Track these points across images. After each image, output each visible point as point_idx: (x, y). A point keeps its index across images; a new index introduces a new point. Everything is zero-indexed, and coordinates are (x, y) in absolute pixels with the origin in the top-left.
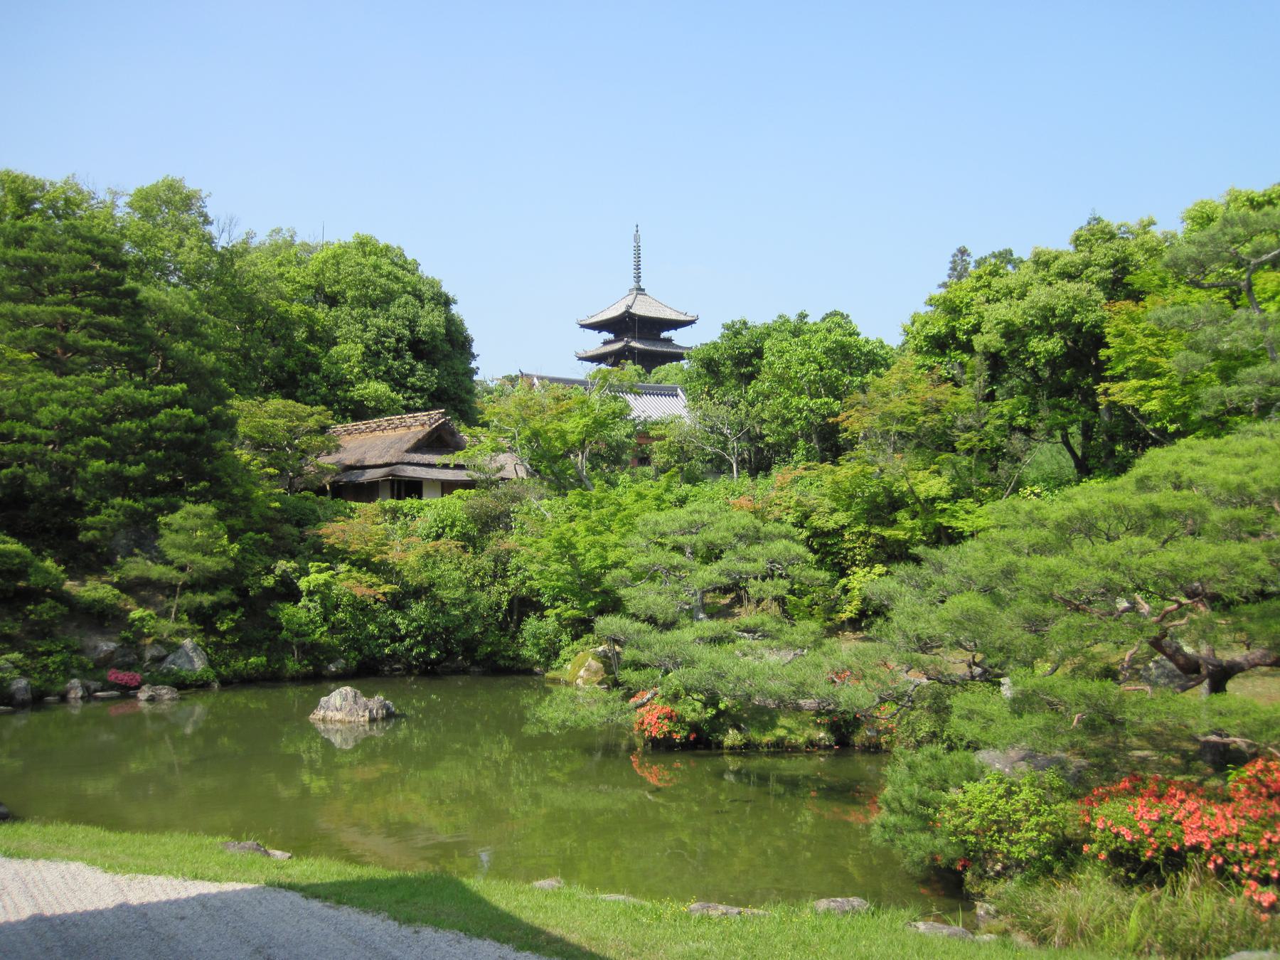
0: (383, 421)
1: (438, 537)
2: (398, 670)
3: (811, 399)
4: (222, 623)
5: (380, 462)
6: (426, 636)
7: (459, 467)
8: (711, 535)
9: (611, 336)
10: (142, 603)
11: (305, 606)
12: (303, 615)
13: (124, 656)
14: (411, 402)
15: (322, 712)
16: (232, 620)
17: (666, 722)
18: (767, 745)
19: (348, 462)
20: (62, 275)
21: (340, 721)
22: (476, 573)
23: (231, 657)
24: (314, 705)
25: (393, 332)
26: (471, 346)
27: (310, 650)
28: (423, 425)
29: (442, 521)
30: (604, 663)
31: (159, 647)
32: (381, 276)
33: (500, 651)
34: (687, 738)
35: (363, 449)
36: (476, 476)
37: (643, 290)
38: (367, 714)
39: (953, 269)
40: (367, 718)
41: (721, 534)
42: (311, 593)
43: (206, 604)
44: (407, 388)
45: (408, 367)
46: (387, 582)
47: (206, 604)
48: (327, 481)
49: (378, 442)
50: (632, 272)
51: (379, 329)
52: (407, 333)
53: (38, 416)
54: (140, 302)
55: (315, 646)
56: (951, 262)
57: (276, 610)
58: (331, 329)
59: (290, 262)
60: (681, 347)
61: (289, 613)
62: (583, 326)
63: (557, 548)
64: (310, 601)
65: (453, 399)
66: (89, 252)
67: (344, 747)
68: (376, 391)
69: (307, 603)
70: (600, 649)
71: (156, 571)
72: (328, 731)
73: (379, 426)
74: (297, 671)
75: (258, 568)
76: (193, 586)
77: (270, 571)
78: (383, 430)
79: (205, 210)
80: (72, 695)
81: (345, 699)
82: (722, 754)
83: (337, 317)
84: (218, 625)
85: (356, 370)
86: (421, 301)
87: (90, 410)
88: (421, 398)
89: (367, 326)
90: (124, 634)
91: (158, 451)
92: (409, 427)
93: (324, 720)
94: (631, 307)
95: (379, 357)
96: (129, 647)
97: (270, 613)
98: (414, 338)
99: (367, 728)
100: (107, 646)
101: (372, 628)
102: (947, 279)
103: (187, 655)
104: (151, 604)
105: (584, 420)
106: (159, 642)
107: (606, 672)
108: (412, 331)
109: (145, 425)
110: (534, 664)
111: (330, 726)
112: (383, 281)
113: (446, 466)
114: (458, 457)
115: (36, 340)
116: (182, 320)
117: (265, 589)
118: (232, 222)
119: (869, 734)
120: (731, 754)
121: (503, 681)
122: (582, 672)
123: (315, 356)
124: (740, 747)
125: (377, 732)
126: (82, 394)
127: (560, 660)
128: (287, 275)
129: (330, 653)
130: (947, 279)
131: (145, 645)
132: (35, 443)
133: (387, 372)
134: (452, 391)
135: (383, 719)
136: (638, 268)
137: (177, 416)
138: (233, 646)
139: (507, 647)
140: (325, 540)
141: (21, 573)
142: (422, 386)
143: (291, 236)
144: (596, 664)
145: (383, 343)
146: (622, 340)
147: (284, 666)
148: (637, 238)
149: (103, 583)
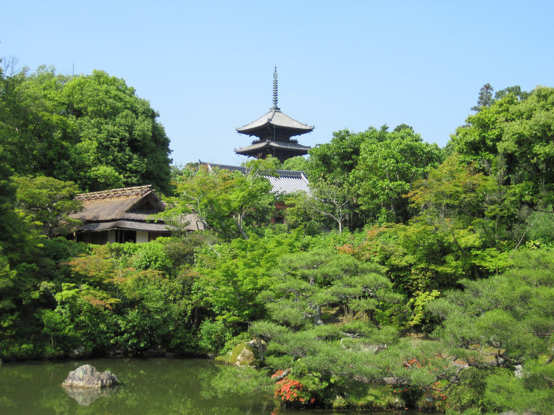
0: (111, 192)
1: (147, 268)
3: (391, 182)
4: (5, 322)
5: (109, 218)
7: (160, 222)
8: (326, 269)
9: (258, 139)
11: (59, 312)
12: (57, 317)
14: (129, 180)
15: (70, 381)
16: (11, 320)
17: (296, 390)
18: (361, 406)
19: (87, 218)
21: (82, 387)
22: (171, 292)
23: (10, 344)
24: (65, 376)
25: (118, 134)
26: (168, 144)
28: (137, 195)
29: (149, 258)
30: (254, 351)
32: (110, 98)
33: (185, 343)
34: (309, 401)
35: (98, 210)
36: (171, 228)
37: (279, 109)
38: (100, 383)
39: (481, 98)
40: (99, 385)
41: (333, 269)
42: (63, 303)
44: (127, 170)
46: (113, 297)
48: (74, 230)
49: (108, 205)
50: (272, 97)
51: (109, 132)
55: (65, 337)
56: (480, 94)
57: (41, 314)
58: (77, 131)
59: (51, 87)
60: (302, 146)
61: (48, 315)
62: (240, 132)
63: (225, 276)
64: (63, 308)
65: (156, 179)
67: (84, 404)
68: (105, 172)
69: (61, 309)
70: (251, 342)
72: (74, 393)
73: (108, 195)
74: (53, 354)
75: (29, 286)
77: (36, 288)
78: (111, 198)
81: (85, 373)
82: (332, 412)
83: (81, 124)
84: (2, 323)
85: (92, 158)
86: (136, 114)
88: (136, 177)
89: (101, 130)
92: (128, 196)
93: (71, 386)
94: (271, 120)
95: (109, 150)
97: (36, 316)
99: (100, 392)
101: (102, 326)
102: (477, 105)
108: (131, 134)
110: (208, 351)
111: (75, 391)
113: (152, 222)
114: (160, 216)
117: (34, 300)
118: (14, 61)
119: (428, 400)
120: (338, 412)
121: (187, 362)
122: (239, 357)
123: (67, 148)
124: (343, 408)
125: (106, 394)
127: (225, 349)
128: (49, 96)
129: (74, 342)
130: (477, 105)
133: (114, 160)
134: (156, 173)
135: (110, 386)
136: (276, 95)
138: (11, 337)
139: (190, 340)
140: (73, 269)
143: (52, 71)
144: (248, 352)
145: (113, 140)
146: (265, 141)
147: (44, 350)
148: (275, 76)
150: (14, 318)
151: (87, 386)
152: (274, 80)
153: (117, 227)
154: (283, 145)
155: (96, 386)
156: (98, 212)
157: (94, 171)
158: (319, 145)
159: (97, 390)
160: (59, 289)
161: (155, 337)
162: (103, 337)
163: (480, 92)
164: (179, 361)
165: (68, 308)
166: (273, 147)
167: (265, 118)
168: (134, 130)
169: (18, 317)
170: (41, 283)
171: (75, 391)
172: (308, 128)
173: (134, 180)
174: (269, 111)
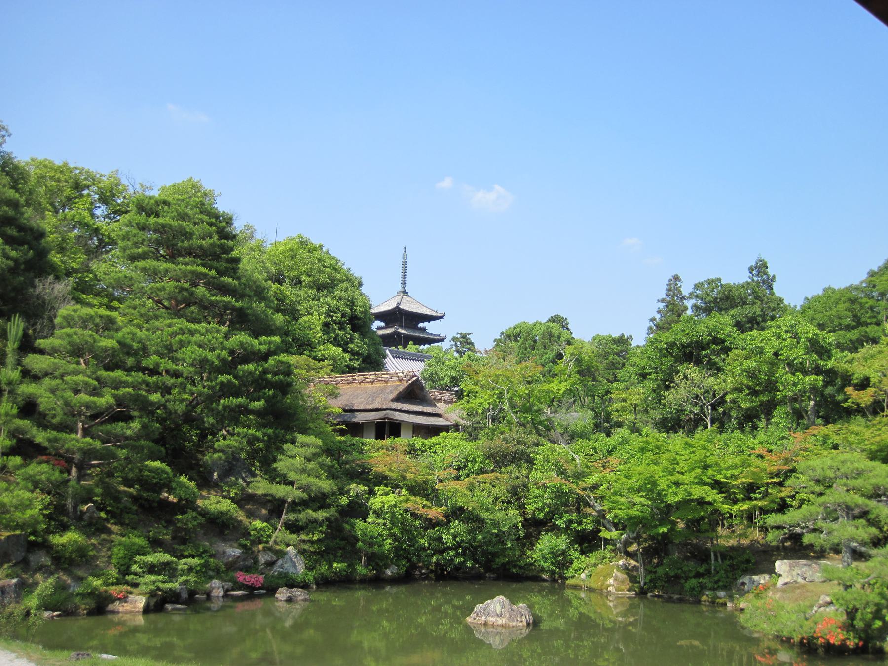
2: (424, 574)
5: (370, 407)
9: (383, 324)
10: (251, 515)
13: (244, 560)
15: (484, 618)
20: (195, 242)
22: (497, 499)
27: (374, 559)
28: (400, 381)
30: (628, 574)
31: (270, 554)
32: (325, 267)
37: (407, 293)
38: (524, 619)
39: (669, 290)
42: (378, 514)
43: (320, 519)
45: (349, 336)
47: (320, 519)
50: (400, 280)
51: (329, 307)
52: (348, 311)
53: (179, 355)
54: (238, 268)
57: (353, 526)
66: (211, 225)
70: (621, 563)
71: (280, 491)
72: (488, 633)
73: (354, 380)
76: (304, 504)
78: (360, 383)
79: (215, 206)
80: (214, 593)
81: (503, 607)
87: (225, 353)
88: (357, 360)
92: (386, 382)
95: (328, 327)
96: (246, 553)
98: (352, 315)
100: (234, 552)
102: (665, 296)
103: (291, 560)
104: (256, 517)
105: (563, 384)
106: (270, 549)
107: (631, 581)
108: (351, 310)
109: (260, 368)
112: (327, 270)
116: (257, 287)
121: (514, 585)
122: (611, 581)
127: (571, 570)
130: (665, 296)
131: (259, 551)
133: (335, 339)
136: (404, 277)
137: (282, 362)
141: (158, 488)
144: (622, 576)
145: (332, 317)
147: (355, 570)
148: (404, 256)
149: (224, 497)
151: (511, 624)
153: (388, 419)
155: (521, 624)
156: (348, 400)
157: (320, 351)
158: (461, 334)
159: (521, 630)
160: (371, 493)
162: (423, 554)
163: (667, 282)
164: (501, 583)
166: (402, 333)
170: (350, 485)
171: (491, 630)
172: (438, 315)
173: (356, 364)
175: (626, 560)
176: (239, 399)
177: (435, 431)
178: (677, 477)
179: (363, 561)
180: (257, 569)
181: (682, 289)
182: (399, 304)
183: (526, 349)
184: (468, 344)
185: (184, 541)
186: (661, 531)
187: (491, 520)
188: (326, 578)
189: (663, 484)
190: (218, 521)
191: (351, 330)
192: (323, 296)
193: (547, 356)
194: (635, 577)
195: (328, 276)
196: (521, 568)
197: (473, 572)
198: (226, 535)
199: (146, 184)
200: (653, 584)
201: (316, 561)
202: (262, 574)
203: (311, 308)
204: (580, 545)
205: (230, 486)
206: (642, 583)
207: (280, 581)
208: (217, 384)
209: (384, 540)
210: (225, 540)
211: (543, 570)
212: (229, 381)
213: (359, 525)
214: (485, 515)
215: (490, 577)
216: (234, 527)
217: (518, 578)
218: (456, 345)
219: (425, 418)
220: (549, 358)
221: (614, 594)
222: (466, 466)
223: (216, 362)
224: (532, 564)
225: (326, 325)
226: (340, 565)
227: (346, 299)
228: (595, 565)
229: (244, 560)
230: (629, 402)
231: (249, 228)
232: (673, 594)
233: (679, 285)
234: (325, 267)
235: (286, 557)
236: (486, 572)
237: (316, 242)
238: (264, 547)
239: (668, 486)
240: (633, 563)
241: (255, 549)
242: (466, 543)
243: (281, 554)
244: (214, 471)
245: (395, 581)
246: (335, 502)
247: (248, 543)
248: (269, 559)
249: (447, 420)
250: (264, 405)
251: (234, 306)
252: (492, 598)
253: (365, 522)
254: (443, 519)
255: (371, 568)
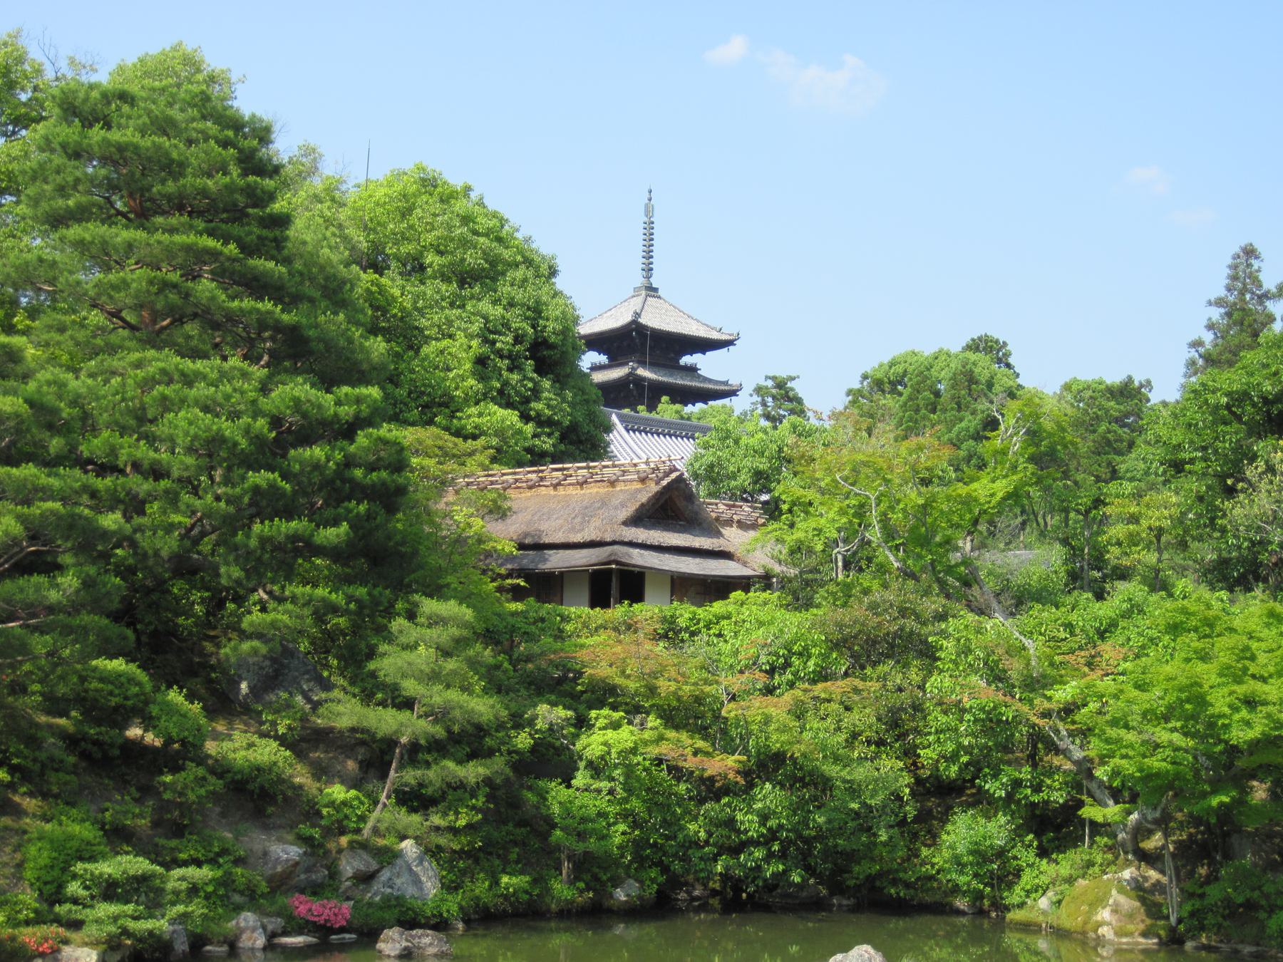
2: (697, 898)
5: (578, 538)
6: (785, 845)
9: (603, 359)
10: (322, 772)
13: (308, 870)
20: (191, 181)
22: (855, 735)
25: (506, 325)
28: (643, 480)
30: (1143, 900)
31: (365, 856)
37: (656, 290)
39: (1234, 278)
42: (597, 769)
45: (530, 385)
47: (472, 780)
50: (639, 262)
51: (486, 318)
52: (531, 331)
53: (161, 429)
54: (287, 239)
56: (1230, 267)
57: (543, 796)
60: (710, 381)
70: (1127, 874)
71: (386, 720)
76: (438, 748)
78: (555, 486)
79: (235, 104)
80: (245, 942)
88: (549, 435)
90: (305, 829)
91: (358, 504)
92: (612, 483)
96: (312, 854)
98: (536, 338)
100: (286, 852)
102: (1222, 292)
103: (411, 870)
106: (364, 846)
107: (1150, 914)
108: (533, 327)
109: (338, 456)
112: (482, 240)
115: (148, 291)
116: (327, 279)
122: (1105, 914)
126: (242, 393)
127: (1017, 889)
130: (1222, 292)
131: (340, 851)
132: (156, 479)
133: (501, 392)
136: (648, 255)
137: (385, 442)
142: (549, 418)
144: (1128, 903)
145: (493, 343)
146: (627, 364)
147: (548, 890)
148: (649, 210)
150: (480, 804)
152: (646, 219)
153: (617, 563)
154: (664, 375)
157: (469, 416)
158: (773, 378)
160: (582, 723)
161: (816, 857)
162: (695, 855)
163: (1229, 261)
165: (621, 779)
166: (644, 379)
167: (623, 310)
168: (541, 317)
169: (487, 801)
170: (535, 706)
172: (724, 337)
173: (547, 444)
174: (632, 293)
175: (1138, 868)
176: (294, 524)
177: (718, 588)
178: (1250, 687)
179: (564, 872)
180: (336, 889)
181: (1262, 276)
182: (638, 315)
183: (917, 411)
184: (790, 400)
185: (178, 831)
186: (1215, 801)
187: (845, 781)
188: (486, 908)
189: (1219, 702)
190: (250, 787)
191: (536, 371)
192: (472, 297)
193: (963, 425)
194: (1159, 905)
195: (484, 253)
196: (908, 885)
197: (804, 894)
198: (269, 816)
199: (80, 58)
200: (1197, 920)
201: (463, 872)
202: (348, 899)
203: (450, 323)
204: (1038, 835)
205: (277, 712)
206: (1173, 920)
207: (387, 915)
208: (245, 492)
209: (609, 825)
210: (266, 828)
211: (956, 889)
212: (272, 486)
213: (557, 794)
214: (831, 770)
215: (840, 906)
216: (286, 799)
217: (901, 908)
218: (764, 404)
219: (698, 560)
220: (967, 429)
221: (1111, 943)
222: (787, 664)
223: (244, 443)
224: (932, 878)
225: (481, 361)
226: (514, 880)
227: (523, 305)
228: (1070, 880)
229: (308, 870)
230: (1144, 523)
231: (309, 151)
232: (1242, 942)
233: (1256, 267)
234: (476, 233)
235: (399, 861)
236: (832, 894)
237: (455, 180)
238: (351, 843)
239: (1230, 706)
240: (1153, 875)
241: (331, 845)
242: (788, 831)
243: (388, 856)
244: (241, 679)
245: (633, 913)
246: (504, 743)
247: (316, 833)
248: (362, 867)
249: (745, 564)
250: (347, 534)
251: (278, 321)
252: (846, 948)
253: (569, 786)
254: (739, 779)
255: (581, 885)
